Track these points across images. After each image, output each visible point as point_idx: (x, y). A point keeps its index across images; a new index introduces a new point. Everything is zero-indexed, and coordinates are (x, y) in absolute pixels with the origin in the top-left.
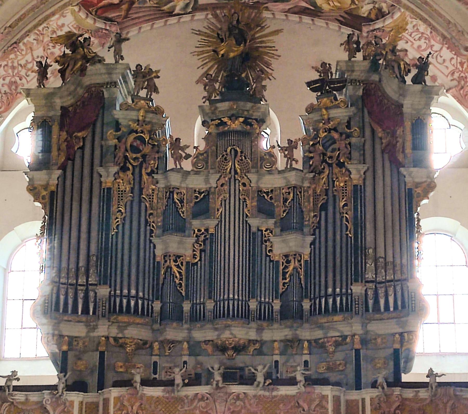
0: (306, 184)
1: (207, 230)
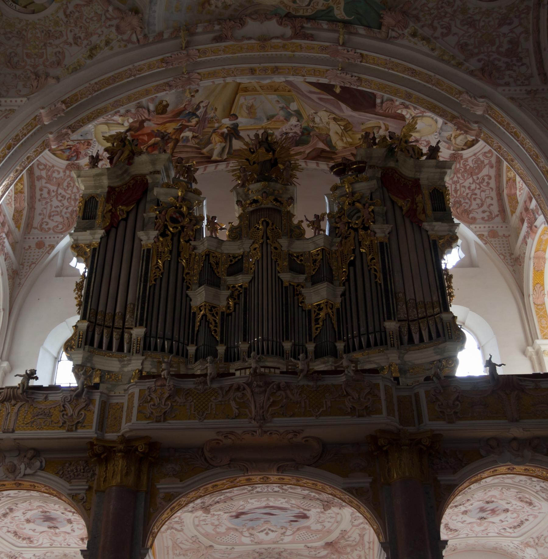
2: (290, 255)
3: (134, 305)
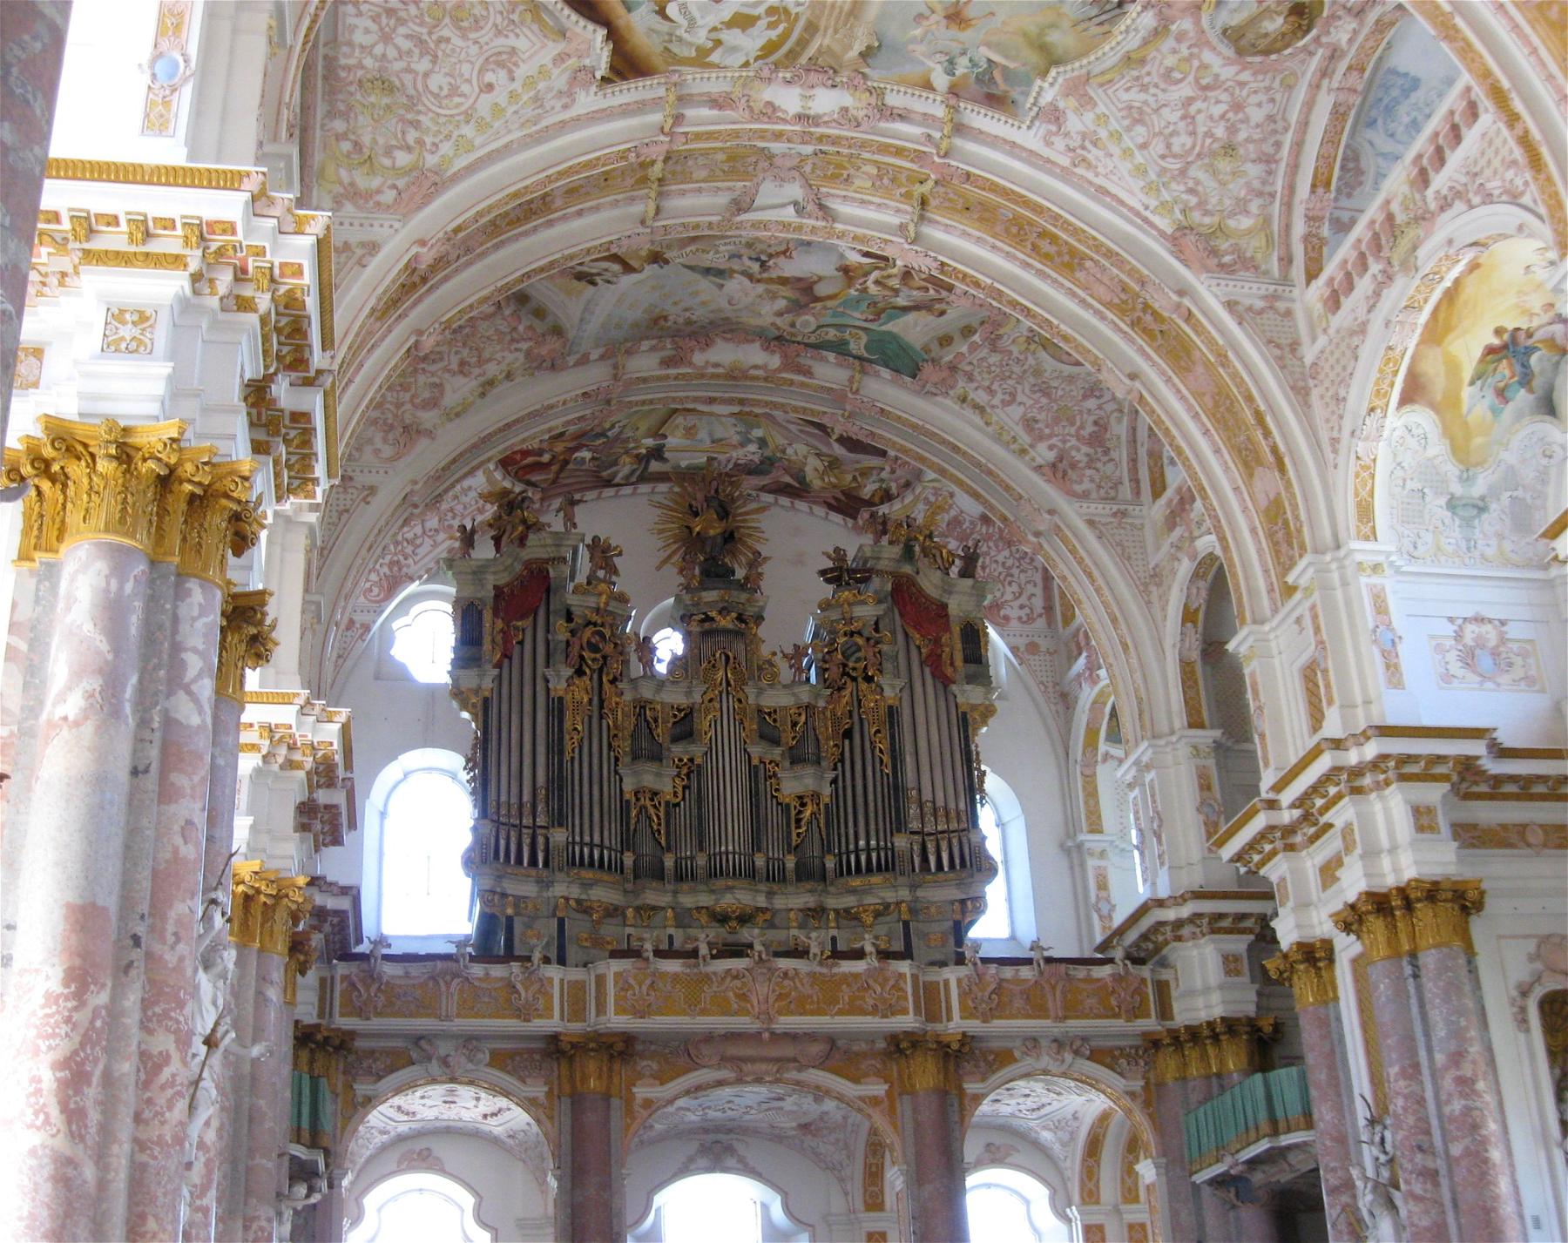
0: (821, 704)
1: (691, 760)
2: (760, 711)
3: (547, 790)
